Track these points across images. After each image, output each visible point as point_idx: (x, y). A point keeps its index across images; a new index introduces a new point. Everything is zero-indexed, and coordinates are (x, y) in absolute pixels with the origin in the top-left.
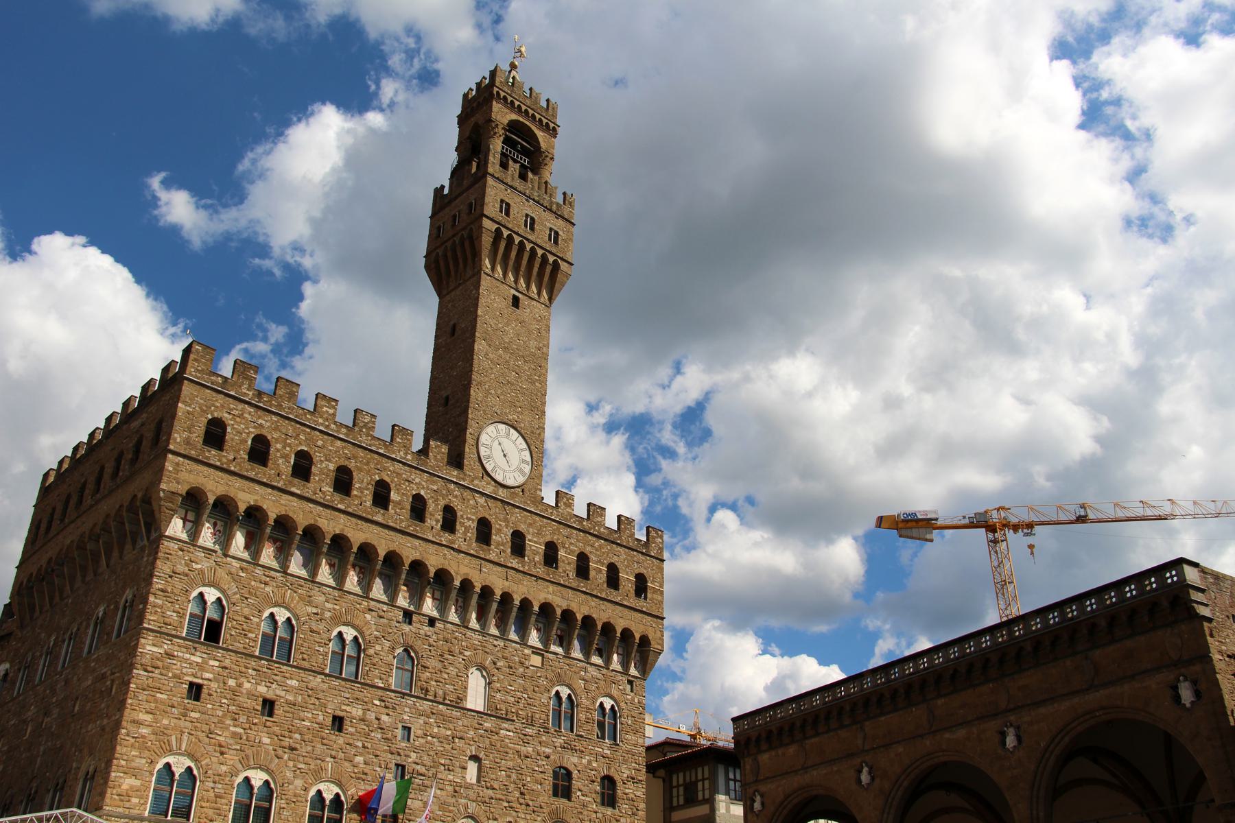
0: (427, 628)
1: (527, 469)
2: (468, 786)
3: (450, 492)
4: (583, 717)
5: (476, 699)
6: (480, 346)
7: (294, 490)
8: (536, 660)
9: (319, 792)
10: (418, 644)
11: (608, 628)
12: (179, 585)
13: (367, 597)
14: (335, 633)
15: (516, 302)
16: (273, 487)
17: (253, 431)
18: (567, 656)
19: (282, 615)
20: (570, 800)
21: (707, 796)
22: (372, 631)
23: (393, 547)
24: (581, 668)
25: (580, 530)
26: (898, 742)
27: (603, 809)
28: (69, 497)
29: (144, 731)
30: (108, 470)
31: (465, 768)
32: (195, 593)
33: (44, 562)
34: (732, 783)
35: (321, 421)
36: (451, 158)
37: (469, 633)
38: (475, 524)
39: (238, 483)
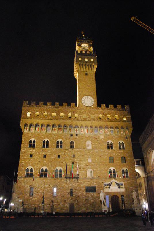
0: (76, 136)
1: (93, 102)
8: (102, 137)
23: (65, 124)
29: (23, 164)
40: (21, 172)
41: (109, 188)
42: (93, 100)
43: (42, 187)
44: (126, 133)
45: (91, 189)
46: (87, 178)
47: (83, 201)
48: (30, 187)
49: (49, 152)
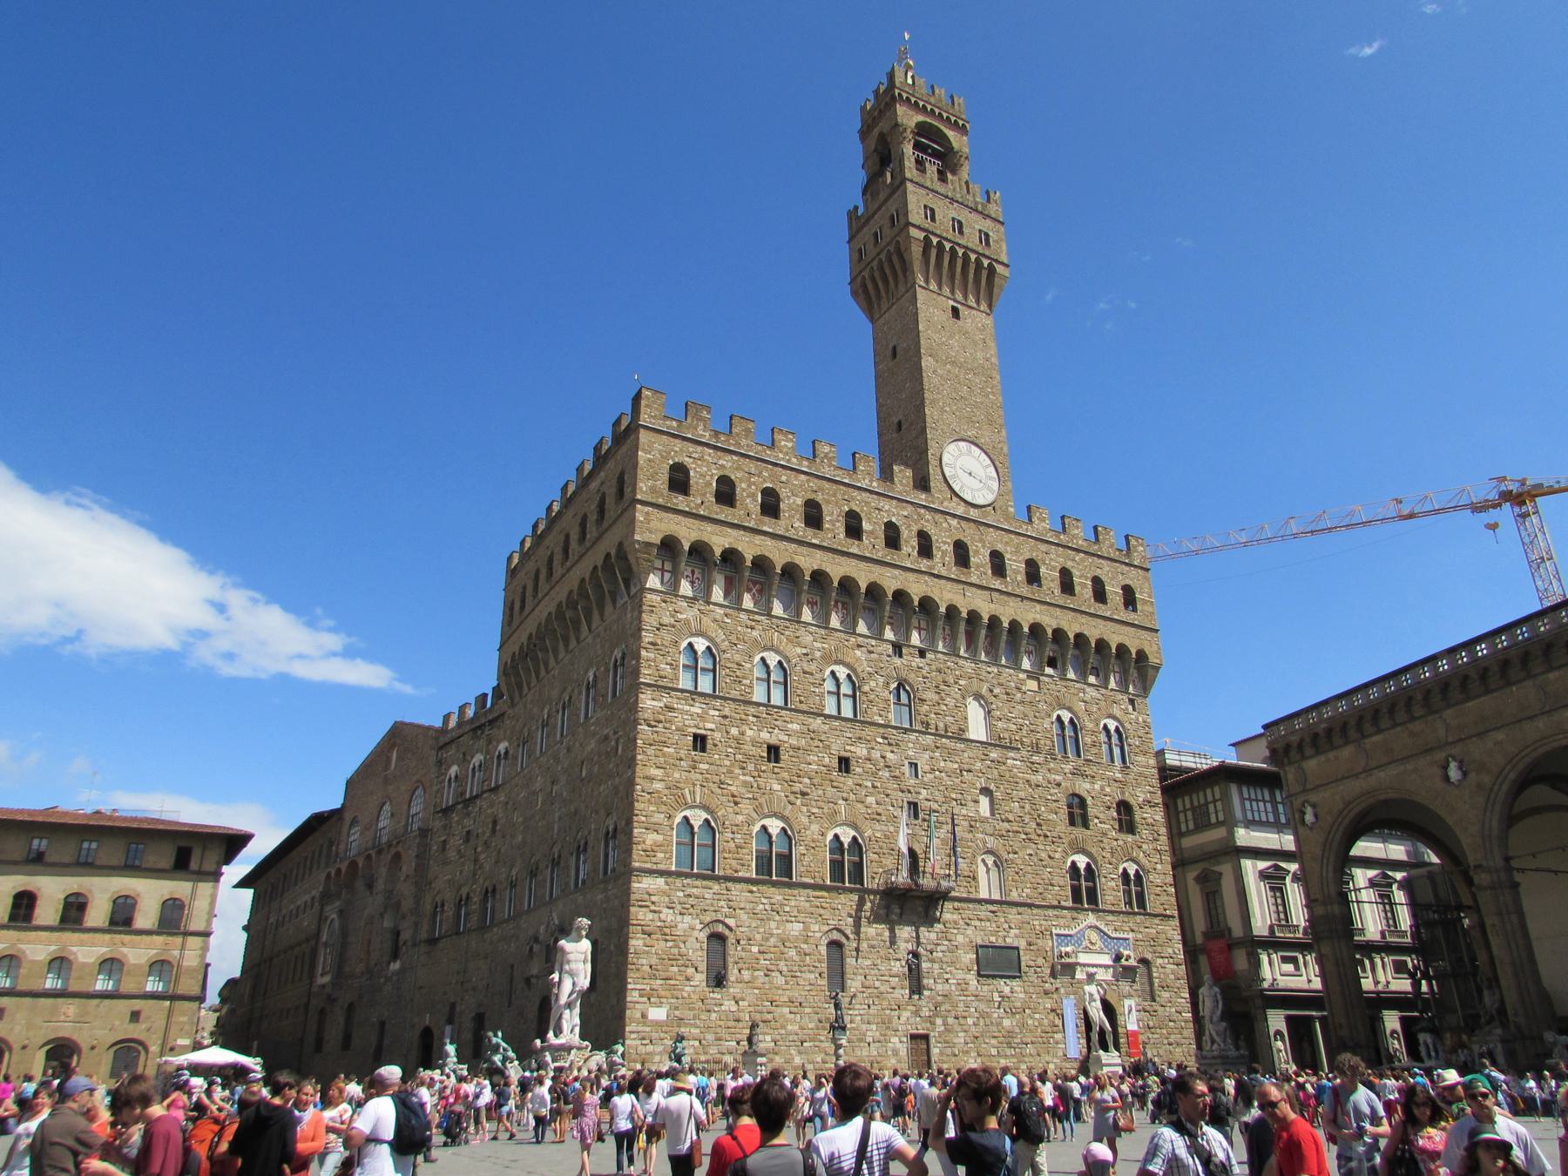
0: (918, 661)
1: (995, 485)
2: (984, 820)
3: (921, 517)
4: (1088, 740)
5: (977, 729)
6: (927, 362)
7: (765, 528)
8: (1032, 685)
9: (836, 836)
10: (912, 677)
11: (1102, 645)
12: (668, 638)
13: (854, 633)
14: (828, 672)
15: (955, 312)
16: (745, 528)
17: (716, 473)
18: (1063, 678)
19: (773, 659)
20: (1086, 825)
21: (1221, 818)
22: (864, 667)
23: (873, 578)
25: (1058, 545)
26: (1498, 728)
27: (1123, 836)
28: (538, 572)
29: (658, 786)
30: (574, 537)
31: (977, 802)
32: (684, 644)
33: (524, 639)
34: (1247, 804)
36: (861, 177)
37: (961, 662)
39: (710, 527)
40: (651, 838)
41: (1076, 953)
43: (767, 939)
45: (997, 962)
46: (980, 901)
47: (970, 1021)
48: (707, 932)
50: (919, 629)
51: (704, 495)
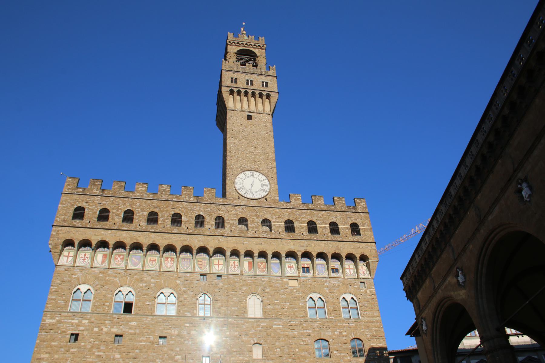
0: (216, 280)
13: (177, 271)
15: (249, 117)
17: (100, 208)
23: (185, 243)
24: (325, 282)
31: (251, 351)
35: (138, 194)
37: (244, 278)
38: (237, 221)
42: (266, 182)
44: (361, 271)
49: (130, 328)
50: (218, 265)
51: (91, 218)
